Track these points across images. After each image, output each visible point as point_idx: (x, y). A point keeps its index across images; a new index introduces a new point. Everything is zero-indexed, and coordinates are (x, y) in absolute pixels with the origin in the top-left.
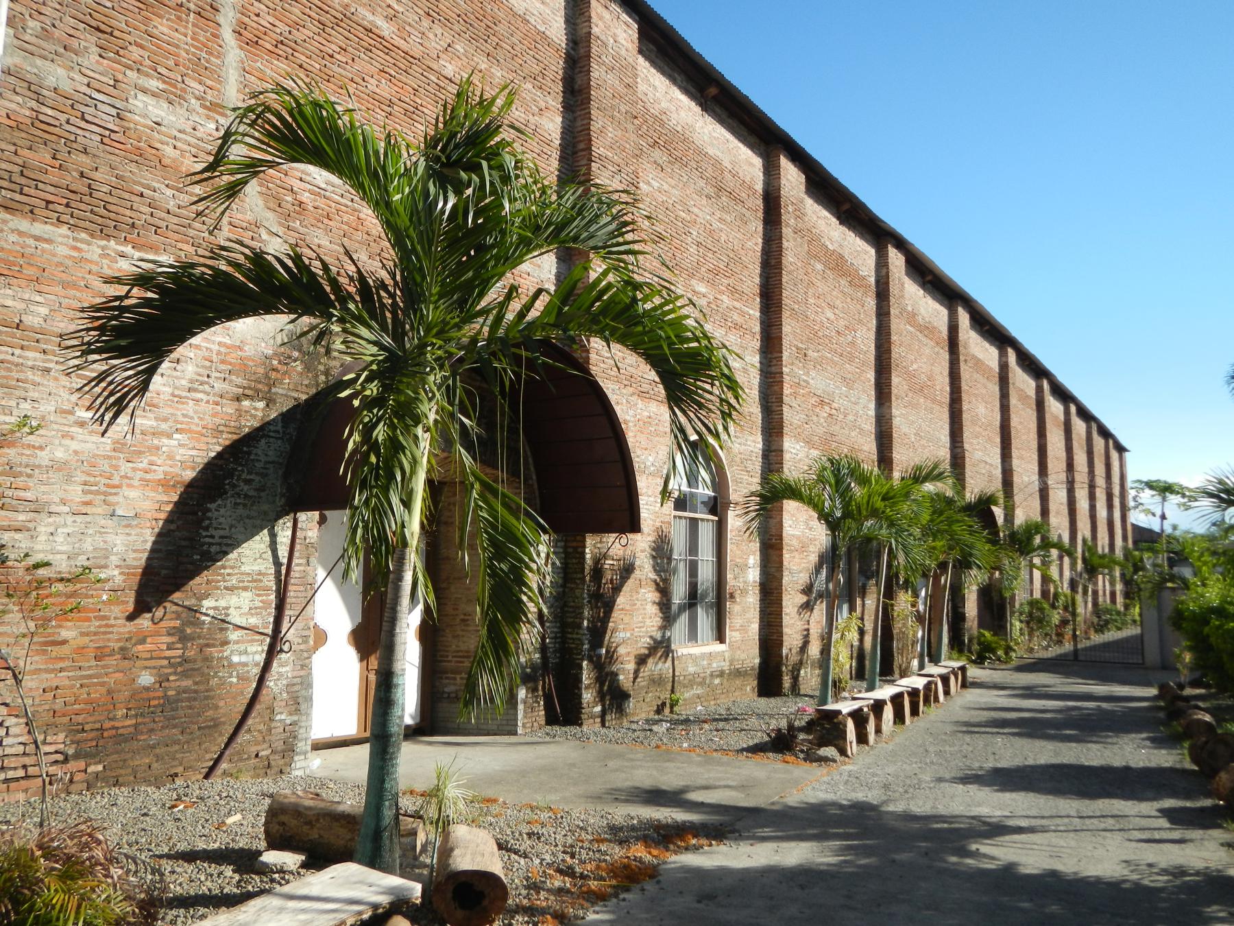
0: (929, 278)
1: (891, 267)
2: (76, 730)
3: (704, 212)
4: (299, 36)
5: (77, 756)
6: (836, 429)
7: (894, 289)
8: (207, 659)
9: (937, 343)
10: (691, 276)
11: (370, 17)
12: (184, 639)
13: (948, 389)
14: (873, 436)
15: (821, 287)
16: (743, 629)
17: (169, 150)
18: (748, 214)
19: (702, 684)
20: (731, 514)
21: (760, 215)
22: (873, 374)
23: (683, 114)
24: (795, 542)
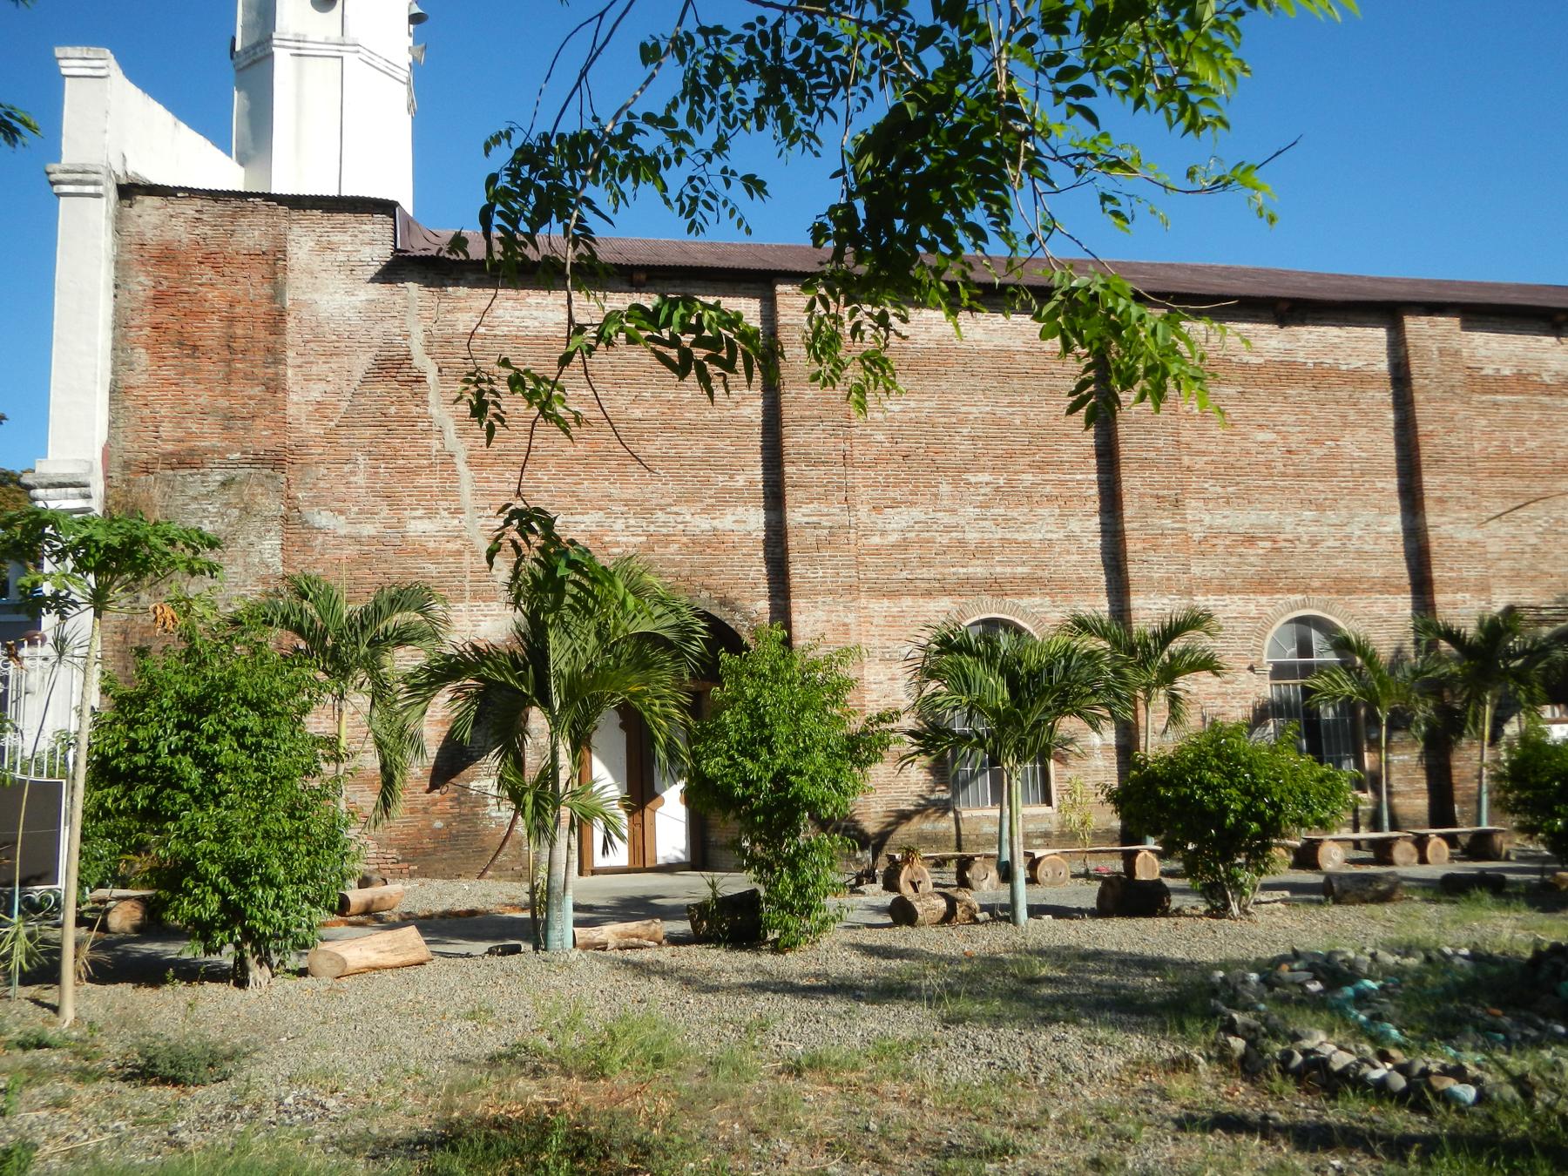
2: (401, 848)
5: (403, 861)
8: (476, 814)
12: (460, 803)
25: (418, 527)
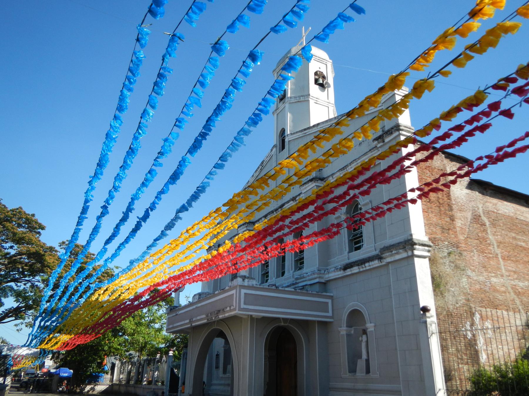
4: (510, 254)
17: (498, 288)
25: (494, 280)
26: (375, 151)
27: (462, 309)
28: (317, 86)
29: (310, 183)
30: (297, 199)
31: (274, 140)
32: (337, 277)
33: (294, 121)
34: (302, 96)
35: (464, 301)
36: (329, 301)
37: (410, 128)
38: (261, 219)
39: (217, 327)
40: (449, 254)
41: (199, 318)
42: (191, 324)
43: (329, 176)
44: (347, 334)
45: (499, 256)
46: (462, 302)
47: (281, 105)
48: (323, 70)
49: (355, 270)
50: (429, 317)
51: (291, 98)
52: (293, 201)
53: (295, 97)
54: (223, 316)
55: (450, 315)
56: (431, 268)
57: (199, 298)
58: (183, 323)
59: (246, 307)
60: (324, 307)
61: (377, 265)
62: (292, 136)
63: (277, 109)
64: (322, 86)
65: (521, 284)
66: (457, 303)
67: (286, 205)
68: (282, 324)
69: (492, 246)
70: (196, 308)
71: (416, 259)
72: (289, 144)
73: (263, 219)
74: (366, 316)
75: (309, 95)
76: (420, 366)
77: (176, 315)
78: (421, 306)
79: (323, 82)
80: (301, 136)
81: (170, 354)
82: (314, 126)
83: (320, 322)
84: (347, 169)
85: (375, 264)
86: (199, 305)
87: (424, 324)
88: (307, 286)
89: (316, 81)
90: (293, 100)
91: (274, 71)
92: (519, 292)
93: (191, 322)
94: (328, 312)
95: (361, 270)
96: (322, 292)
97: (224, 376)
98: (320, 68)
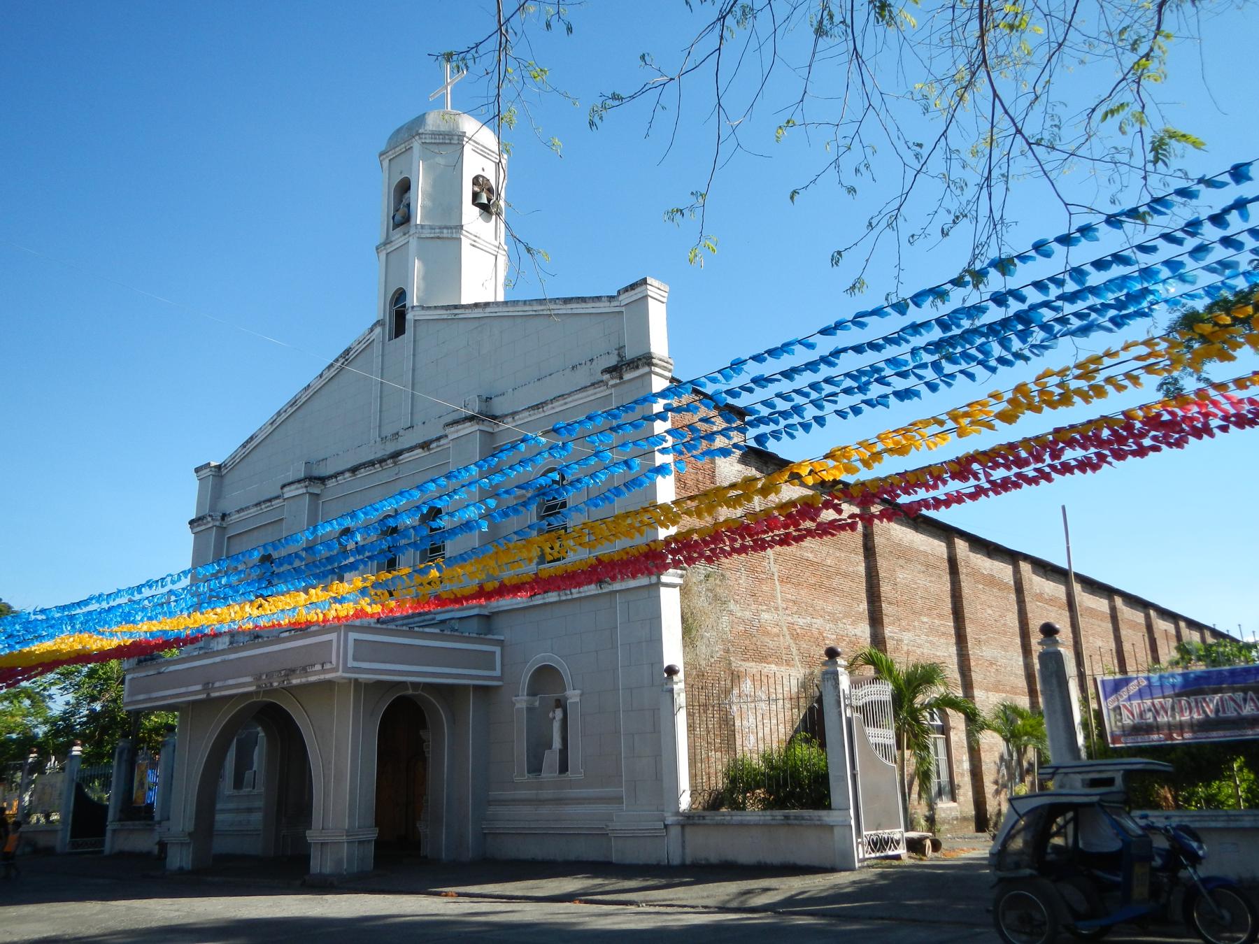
0: (1049, 568)
1: (1022, 573)
3: (922, 581)
6: (1000, 677)
7: (1026, 586)
9: (1060, 607)
10: (921, 615)
11: (806, 554)
13: (1071, 635)
14: (1024, 677)
15: (983, 597)
16: (965, 795)
17: (769, 628)
18: (941, 573)
19: (948, 823)
20: (952, 734)
21: (948, 571)
22: (1019, 639)
23: (908, 536)
24: (986, 746)
26: (602, 388)
27: (718, 665)
28: (477, 210)
29: (468, 424)
30: (431, 447)
31: (375, 309)
32: (515, 607)
33: (426, 277)
34: (447, 228)
35: (722, 653)
36: (497, 650)
37: (667, 363)
38: (342, 473)
39: (264, 699)
40: (707, 576)
41: (231, 682)
42: (208, 694)
43: (506, 416)
44: (527, 708)
45: (776, 578)
46: (718, 655)
47: (398, 238)
48: (490, 175)
49: (552, 597)
50: (677, 683)
51: (422, 227)
52: (423, 448)
53: (432, 228)
54: (304, 680)
55: (701, 675)
56: (682, 602)
57: (231, 643)
58: (183, 690)
59: (356, 664)
60: (486, 660)
61: (593, 593)
62: (423, 312)
63: (387, 242)
64: (485, 209)
65: (801, 621)
66: (712, 657)
67: (407, 455)
68: (410, 692)
69: (767, 561)
70: (223, 662)
71: (663, 590)
72: (415, 327)
73: (347, 475)
74: (567, 678)
75: (461, 227)
76: (657, 756)
77: (160, 673)
78: (665, 665)
79: (489, 200)
80: (445, 317)
81: (74, 753)
82: (476, 305)
83: (476, 687)
84: (545, 408)
85: (590, 591)
86: (233, 656)
87: (668, 693)
88: (453, 621)
89: (475, 196)
90: (426, 233)
91: (381, 154)
92: (798, 634)
93: (207, 686)
94: (494, 669)
95: (564, 598)
96: (486, 635)
97: (235, 792)
98: (483, 170)
